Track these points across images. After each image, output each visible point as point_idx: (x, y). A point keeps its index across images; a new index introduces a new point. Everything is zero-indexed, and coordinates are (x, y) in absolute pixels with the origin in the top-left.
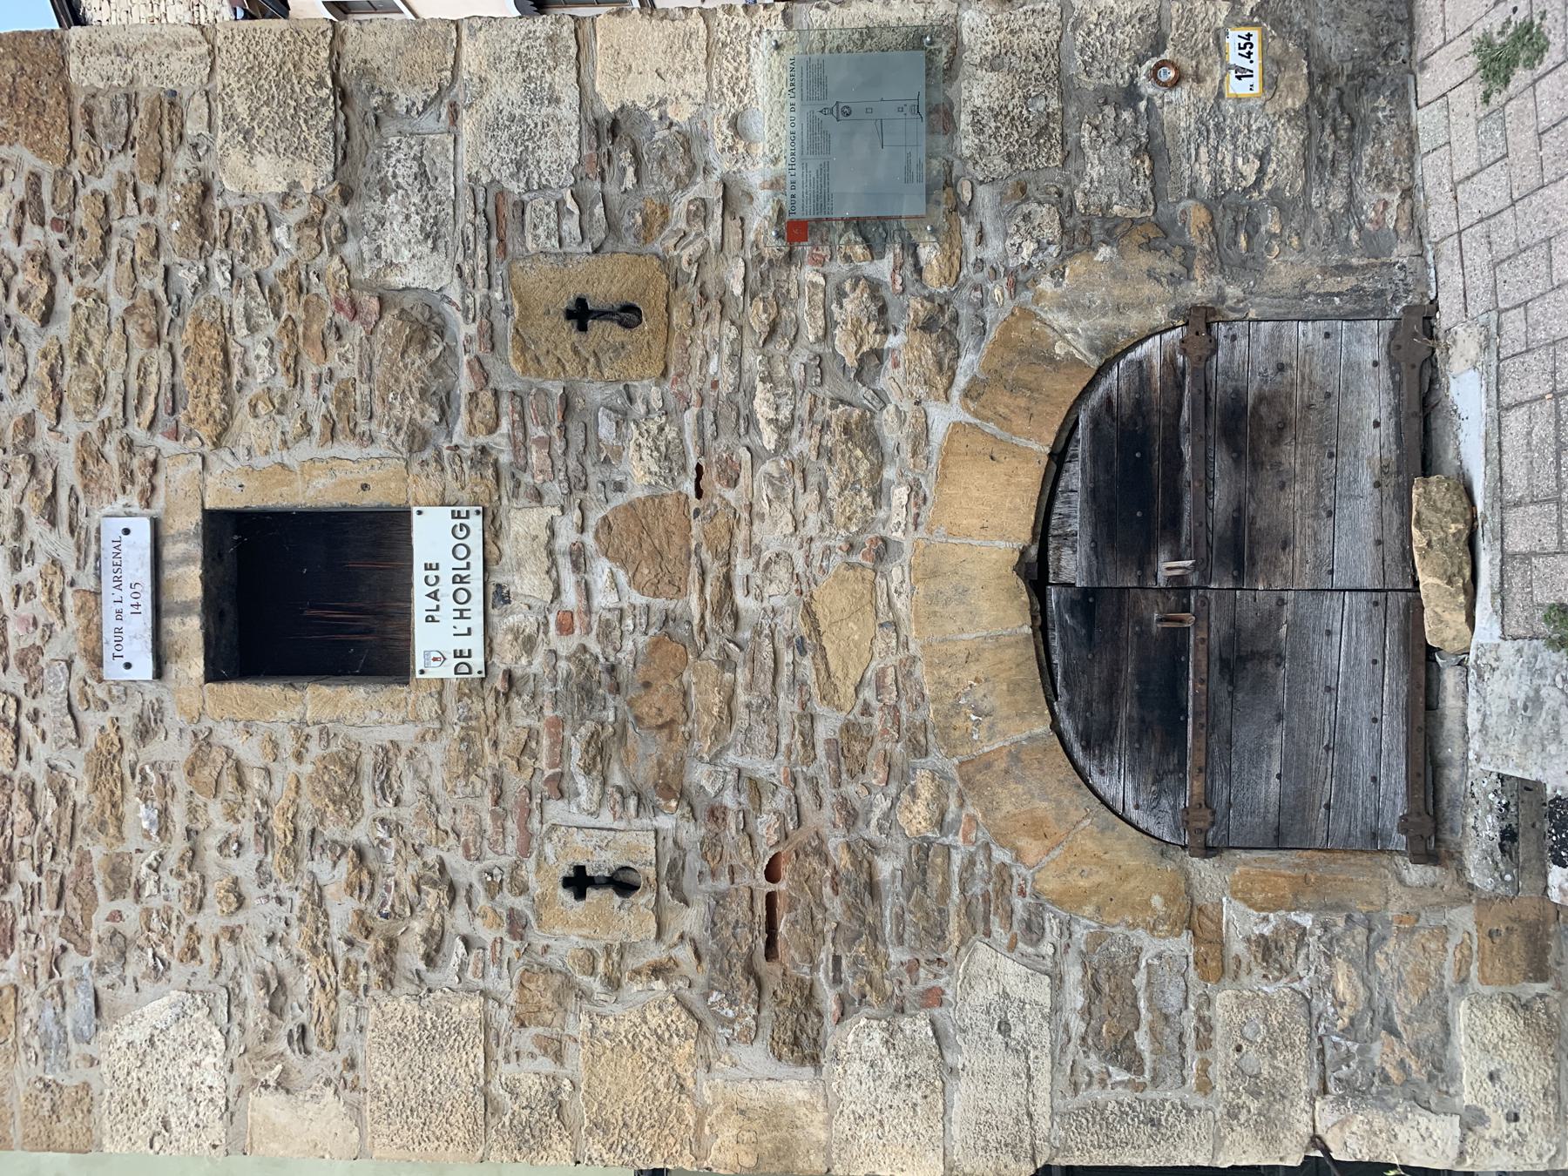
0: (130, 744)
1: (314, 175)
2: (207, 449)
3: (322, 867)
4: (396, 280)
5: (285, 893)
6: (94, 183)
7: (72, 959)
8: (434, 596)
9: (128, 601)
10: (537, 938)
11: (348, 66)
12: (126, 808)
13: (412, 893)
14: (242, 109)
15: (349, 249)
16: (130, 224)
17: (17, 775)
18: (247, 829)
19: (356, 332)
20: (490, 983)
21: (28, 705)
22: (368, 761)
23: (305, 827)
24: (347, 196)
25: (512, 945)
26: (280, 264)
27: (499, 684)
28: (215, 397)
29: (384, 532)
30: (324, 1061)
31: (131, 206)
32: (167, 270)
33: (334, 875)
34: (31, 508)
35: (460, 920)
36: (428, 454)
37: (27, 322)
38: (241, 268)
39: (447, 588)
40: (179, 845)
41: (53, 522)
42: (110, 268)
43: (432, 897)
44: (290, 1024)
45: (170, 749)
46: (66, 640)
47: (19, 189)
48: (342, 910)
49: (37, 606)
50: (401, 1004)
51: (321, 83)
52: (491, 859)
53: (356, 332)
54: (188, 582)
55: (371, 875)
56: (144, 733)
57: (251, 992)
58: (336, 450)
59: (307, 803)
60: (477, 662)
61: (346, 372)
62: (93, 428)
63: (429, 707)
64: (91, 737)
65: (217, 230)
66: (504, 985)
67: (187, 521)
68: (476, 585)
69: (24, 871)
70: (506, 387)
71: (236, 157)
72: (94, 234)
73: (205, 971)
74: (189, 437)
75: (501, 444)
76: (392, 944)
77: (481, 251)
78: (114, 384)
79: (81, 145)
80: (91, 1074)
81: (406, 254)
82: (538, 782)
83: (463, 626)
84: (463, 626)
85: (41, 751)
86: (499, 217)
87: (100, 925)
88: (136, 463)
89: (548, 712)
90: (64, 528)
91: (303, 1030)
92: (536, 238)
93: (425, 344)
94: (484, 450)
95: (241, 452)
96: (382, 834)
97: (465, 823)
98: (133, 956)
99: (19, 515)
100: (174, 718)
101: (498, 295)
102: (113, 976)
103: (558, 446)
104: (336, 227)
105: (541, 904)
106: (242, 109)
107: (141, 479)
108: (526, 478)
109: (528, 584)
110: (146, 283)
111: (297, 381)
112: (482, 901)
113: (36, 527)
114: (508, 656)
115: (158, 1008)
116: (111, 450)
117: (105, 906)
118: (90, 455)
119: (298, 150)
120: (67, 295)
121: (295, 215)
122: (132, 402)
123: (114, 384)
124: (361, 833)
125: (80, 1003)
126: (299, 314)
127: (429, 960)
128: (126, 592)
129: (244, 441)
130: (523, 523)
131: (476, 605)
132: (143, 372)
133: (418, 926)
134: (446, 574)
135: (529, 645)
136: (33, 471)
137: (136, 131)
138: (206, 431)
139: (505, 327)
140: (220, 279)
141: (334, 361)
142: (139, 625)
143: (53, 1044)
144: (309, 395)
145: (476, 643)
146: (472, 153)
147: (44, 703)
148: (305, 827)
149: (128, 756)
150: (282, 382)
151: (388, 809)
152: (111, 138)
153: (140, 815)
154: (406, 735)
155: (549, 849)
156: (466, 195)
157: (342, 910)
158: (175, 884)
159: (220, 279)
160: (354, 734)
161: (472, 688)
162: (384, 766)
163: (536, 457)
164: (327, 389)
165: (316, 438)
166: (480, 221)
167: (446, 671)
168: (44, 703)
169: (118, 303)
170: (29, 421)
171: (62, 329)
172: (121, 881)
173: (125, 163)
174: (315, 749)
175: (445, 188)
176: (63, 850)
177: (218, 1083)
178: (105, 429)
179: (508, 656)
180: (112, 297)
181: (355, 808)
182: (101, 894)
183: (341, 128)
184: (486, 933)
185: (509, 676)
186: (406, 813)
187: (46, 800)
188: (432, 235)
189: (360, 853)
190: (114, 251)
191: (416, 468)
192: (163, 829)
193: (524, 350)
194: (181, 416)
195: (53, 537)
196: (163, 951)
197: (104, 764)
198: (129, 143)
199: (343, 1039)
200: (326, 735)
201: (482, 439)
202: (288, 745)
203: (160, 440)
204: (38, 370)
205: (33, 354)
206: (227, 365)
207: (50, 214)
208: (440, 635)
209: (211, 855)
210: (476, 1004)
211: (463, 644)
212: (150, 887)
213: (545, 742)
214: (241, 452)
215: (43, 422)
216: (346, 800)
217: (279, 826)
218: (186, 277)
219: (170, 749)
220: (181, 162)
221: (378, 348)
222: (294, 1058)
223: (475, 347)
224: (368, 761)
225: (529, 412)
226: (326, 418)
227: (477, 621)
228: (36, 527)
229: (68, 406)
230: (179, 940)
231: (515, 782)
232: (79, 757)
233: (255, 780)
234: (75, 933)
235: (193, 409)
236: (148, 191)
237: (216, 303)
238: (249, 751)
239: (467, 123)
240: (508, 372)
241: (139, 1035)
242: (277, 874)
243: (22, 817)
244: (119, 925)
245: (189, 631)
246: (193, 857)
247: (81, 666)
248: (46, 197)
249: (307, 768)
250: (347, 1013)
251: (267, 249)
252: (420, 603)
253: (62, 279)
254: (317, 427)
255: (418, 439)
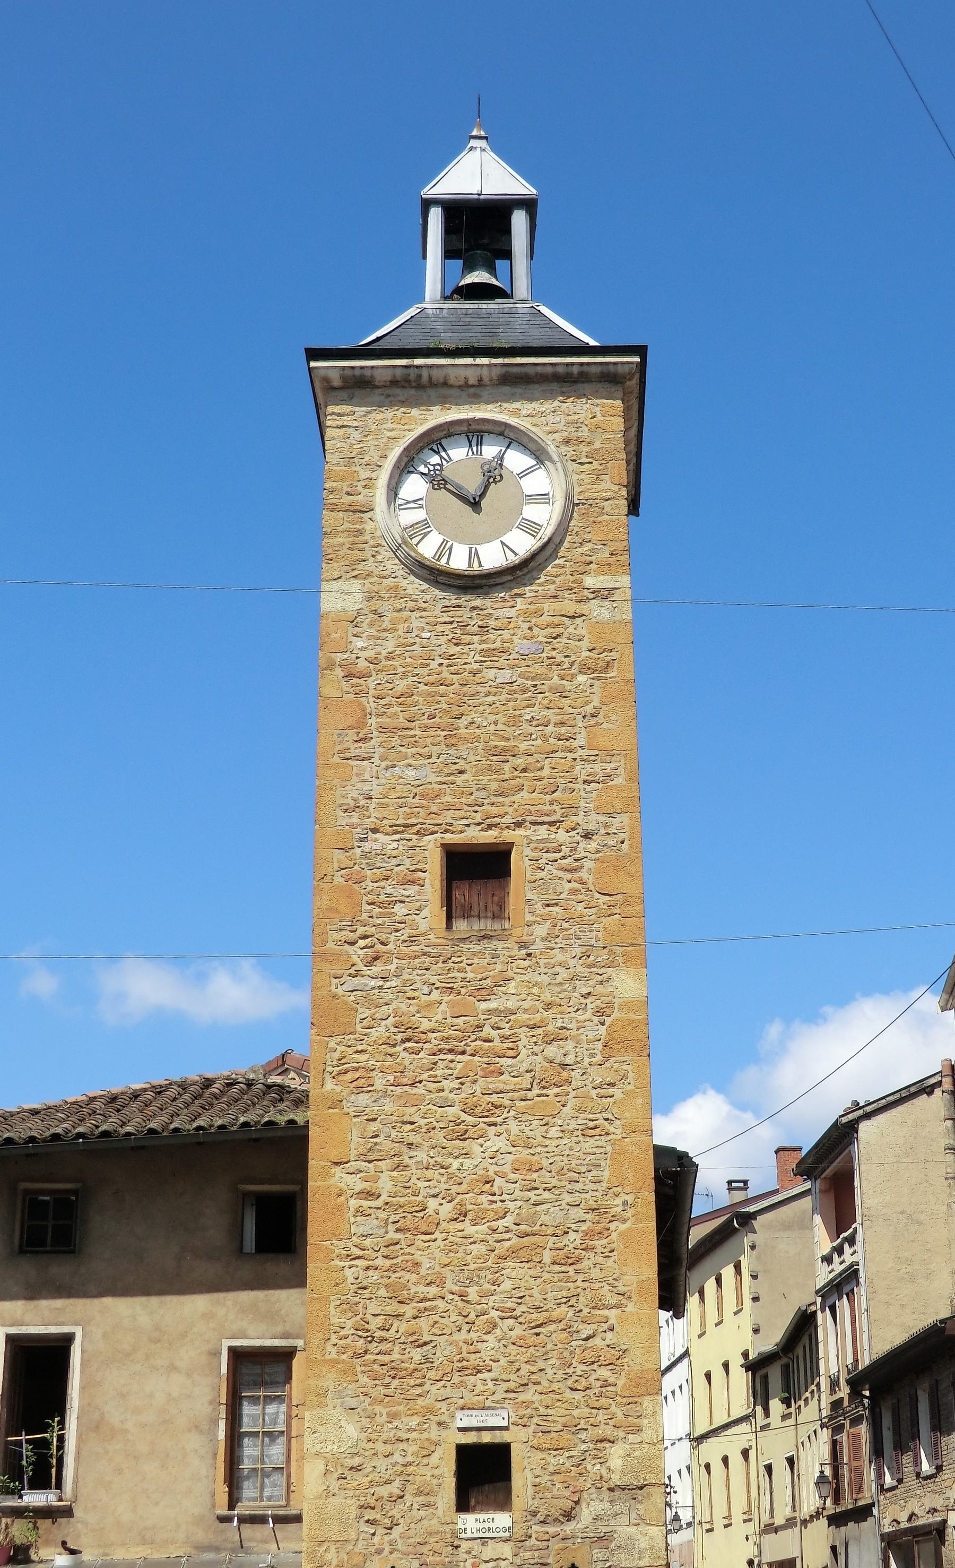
0: (436, 1418)
1: (616, 1479)
2: (530, 1443)
3: (397, 1484)
4: (584, 1505)
5: (389, 1472)
6: (613, 1404)
7: (368, 1400)
8: (484, 1521)
9: (481, 1419)
10: (376, 1558)
11: (652, 1489)
12: (415, 1417)
13: (389, 1515)
14: (637, 1454)
15: (593, 1490)
16: (601, 1416)
17: (426, 1380)
18: (409, 1459)
19: (567, 1493)
20: (361, 1542)
21: (448, 1384)
22: (432, 1499)
23: (410, 1478)
24: (611, 1490)
25: (373, 1549)
26: (589, 1467)
27: (455, 1544)
28: (547, 1446)
29: (504, 1503)
30: (335, 1486)
31: (606, 1417)
32: (586, 1430)
33: (395, 1488)
34: (512, 1385)
35: (381, 1531)
36: (529, 1518)
37: (570, 1383)
38: (588, 1454)
39: (486, 1525)
40: (404, 1436)
41: (507, 1391)
42: (587, 1410)
43: (387, 1522)
44: (347, 1474)
45: (434, 1433)
46: (470, 1398)
47: (612, 1380)
48: (384, 1491)
49: (480, 1387)
50: (354, 1512)
51: (645, 1480)
52: (400, 1541)
53: (567, 1493)
54: (486, 1438)
55: (395, 1501)
56: (440, 1424)
57: (356, 1461)
58: (530, 1486)
59: (418, 1479)
60: (463, 1536)
61: (555, 1492)
62: (536, 1405)
63: (448, 1520)
64: (439, 1405)
65: (599, 1445)
66: (360, 1547)
67: (505, 1437)
68: (487, 1535)
69: (396, 1383)
70: (550, 1543)
71: (622, 1452)
72: (597, 1405)
73: (364, 1445)
74: (534, 1437)
75: (533, 1541)
76: (373, 1508)
77: (592, 1535)
78: (550, 1412)
79: (625, 1400)
80: (330, 1407)
81: (592, 1509)
82: (425, 1557)
83: (474, 1531)
84: (474, 1531)
85: (434, 1388)
86: (603, 1540)
87: (378, 1409)
88: (526, 1419)
89: (447, 1560)
90: (504, 1395)
91: (345, 1478)
92: (597, 1553)
93: (564, 1516)
94: (530, 1537)
95: (529, 1454)
96: (408, 1504)
97: (412, 1532)
98: (368, 1420)
99: (509, 1381)
100: (444, 1433)
101: (579, 1540)
102: (362, 1413)
103: (532, 1562)
104: (600, 1486)
105: (386, 1559)
106: (637, 1454)
107: (520, 1421)
108: (521, 1550)
109: (489, 1552)
110: (582, 1421)
111: (552, 1474)
112: (387, 1538)
113: (505, 1386)
114: (465, 1545)
115: (352, 1431)
116: (529, 1410)
117: (384, 1411)
118: (527, 1404)
119: (623, 1473)
120: (578, 1396)
121: (604, 1472)
122: (544, 1418)
123: (550, 1412)
124: (408, 1498)
125: (353, 1403)
126: (573, 1474)
127: (367, 1521)
128: (484, 1418)
129: (532, 1455)
130: (507, 1550)
131: (481, 1535)
132: (554, 1421)
133: (378, 1517)
134: (491, 1525)
135: (469, 1552)
136: (522, 1385)
137: (630, 1418)
138: (535, 1443)
139: (569, 1543)
140: (584, 1447)
141: (558, 1486)
142: (475, 1424)
143: (340, 1395)
144: (547, 1478)
145: (469, 1535)
146: (624, 1530)
147: (449, 1389)
148: (410, 1478)
149: (432, 1417)
150: (551, 1469)
151: (416, 1506)
152: (627, 1411)
153: (414, 1422)
154: (440, 1512)
155: (403, 1561)
156: (609, 1529)
157: (384, 1491)
158: (391, 1435)
159: (584, 1447)
160: (440, 1495)
161: (454, 1534)
162: (428, 1505)
163: (528, 1555)
164: (549, 1483)
165: (534, 1480)
166: (602, 1534)
167: (460, 1525)
168: (449, 1389)
169: (576, 1413)
170: (539, 1383)
171: (568, 1394)
172: (393, 1416)
173: (620, 1415)
174: (435, 1481)
175: (612, 1522)
176: (402, 1396)
177: (328, 1450)
178: (536, 1409)
179: (465, 1545)
180: (578, 1411)
181: (416, 1495)
182: (388, 1410)
183: (631, 1487)
184: (376, 1539)
185: (457, 1547)
186: (415, 1512)
187: (418, 1391)
188: (597, 1518)
189: (402, 1497)
190: (593, 1411)
191: (525, 1513)
192: (409, 1430)
193: (562, 1550)
194: (541, 1434)
195: (502, 1391)
196: (370, 1431)
197: (430, 1410)
198: (626, 1416)
199: (342, 1492)
200: (439, 1485)
201: (534, 1536)
202: (436, 1472)
203: (533, 1427)
204: (555, 1386)
205: (560, 1385)
206: (557, 1449)
207: (604, 1390)
208: (471, 1522)
209: (402, 1446)
210: (354, 1537)
211: (469, 1531)
212: (390, 1426)
213: (438, 1559)
214: (529, 1454)
215: (539, 1388)
216: (419, 1493)
217: (410, 1469)
218: (583, 1435)
219: (434, 1433)
220: (621, 1434)
221: (562, 1500)
222: (336, 1476)
223: (562, 1533)
224: (432, 1499)
225: (542, 1552)
226: (540, 1484)
227: (475, 1535)
228: (505, 1386)
229: (543, 1396)
230: (373, 1436)
231: (425, 1549)
232: (432, 1401)
233: (425, 1461)
234: (375, 1401)
235: (541, 1440)
236: (611, 1422)
237: (575, 1445)
238: (434, 1459)
239: (633, 1529)
240: (556, 1545)
241: (343, 1423)
242: (395, 1468)
243: (412, 1382)
244: (378, 1415)
245: (470, 1438)
246: (400, 1440)
247: (461, 1402)
248: (609, 1388)
249: (428, 1478)
250: (351, 1493)
251: (593, 1462)
252: (482, 1516)
253: (583, 1394)
254: (538, 1480)
255: (534, 1514)
